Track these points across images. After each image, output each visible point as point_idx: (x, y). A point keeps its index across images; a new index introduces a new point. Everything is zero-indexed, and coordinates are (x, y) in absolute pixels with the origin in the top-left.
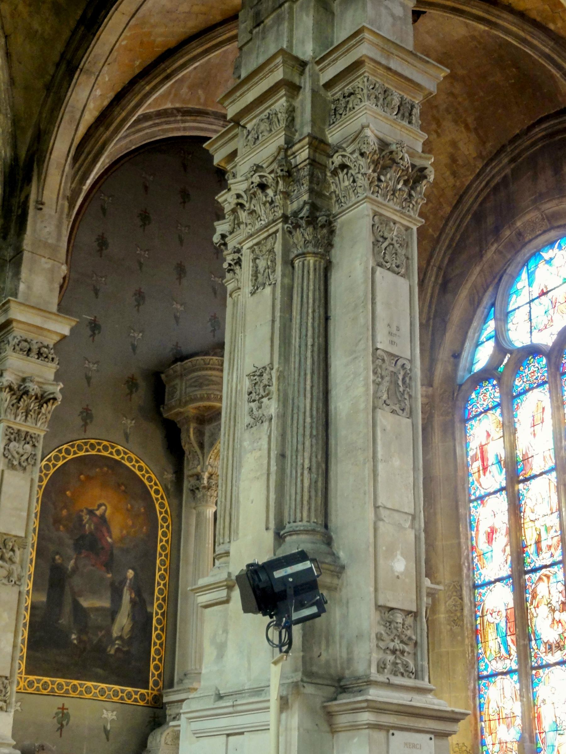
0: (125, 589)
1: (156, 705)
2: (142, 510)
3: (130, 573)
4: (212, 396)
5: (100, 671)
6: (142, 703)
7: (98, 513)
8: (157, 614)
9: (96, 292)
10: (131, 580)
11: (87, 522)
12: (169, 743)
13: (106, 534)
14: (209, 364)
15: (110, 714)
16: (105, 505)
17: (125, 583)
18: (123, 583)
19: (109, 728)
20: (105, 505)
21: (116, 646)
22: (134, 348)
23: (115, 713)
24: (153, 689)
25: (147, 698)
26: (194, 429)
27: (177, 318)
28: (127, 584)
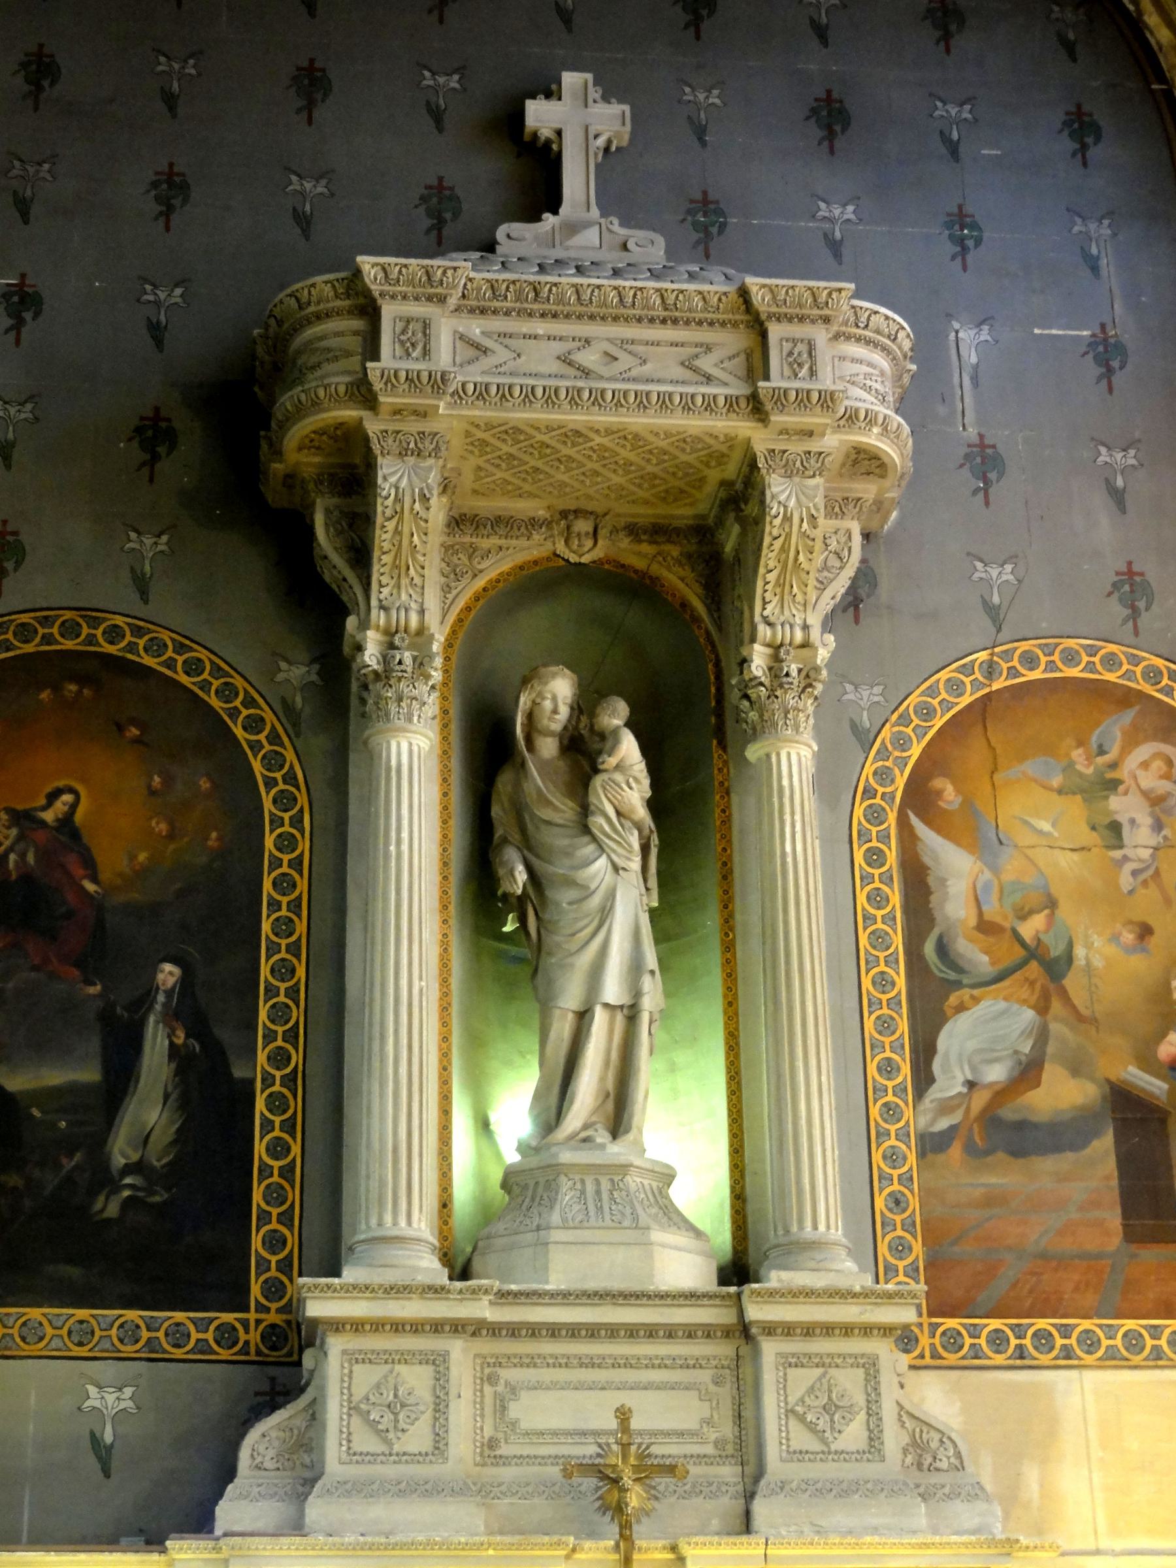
0: (152, 1019)
1: (274, 1356)
2: (205, 784)
3: (168, 974)
4: (321, 393)
5: (73, 1272)
6: (224, 1354)
7: (48, 816)
8: (268, 1080)
9: (23, 208)
10: (169, 993)
11: (11, 849)
12: (269, 1464)
13: (79, 872)
14: (309, 303)
15: (110, 1398)
16: (71, 790)
17: (150, 1008)
18: (143, 1002)
19: (108, 1437)
20: (71, 790)
21: (126, 1193)
22: (156, 331)
23: (128, 1391)
24: (261, 1308)
25: (242, 1337)
26: (328, 512)
27: (303, 222)
28: (158, 1007)
